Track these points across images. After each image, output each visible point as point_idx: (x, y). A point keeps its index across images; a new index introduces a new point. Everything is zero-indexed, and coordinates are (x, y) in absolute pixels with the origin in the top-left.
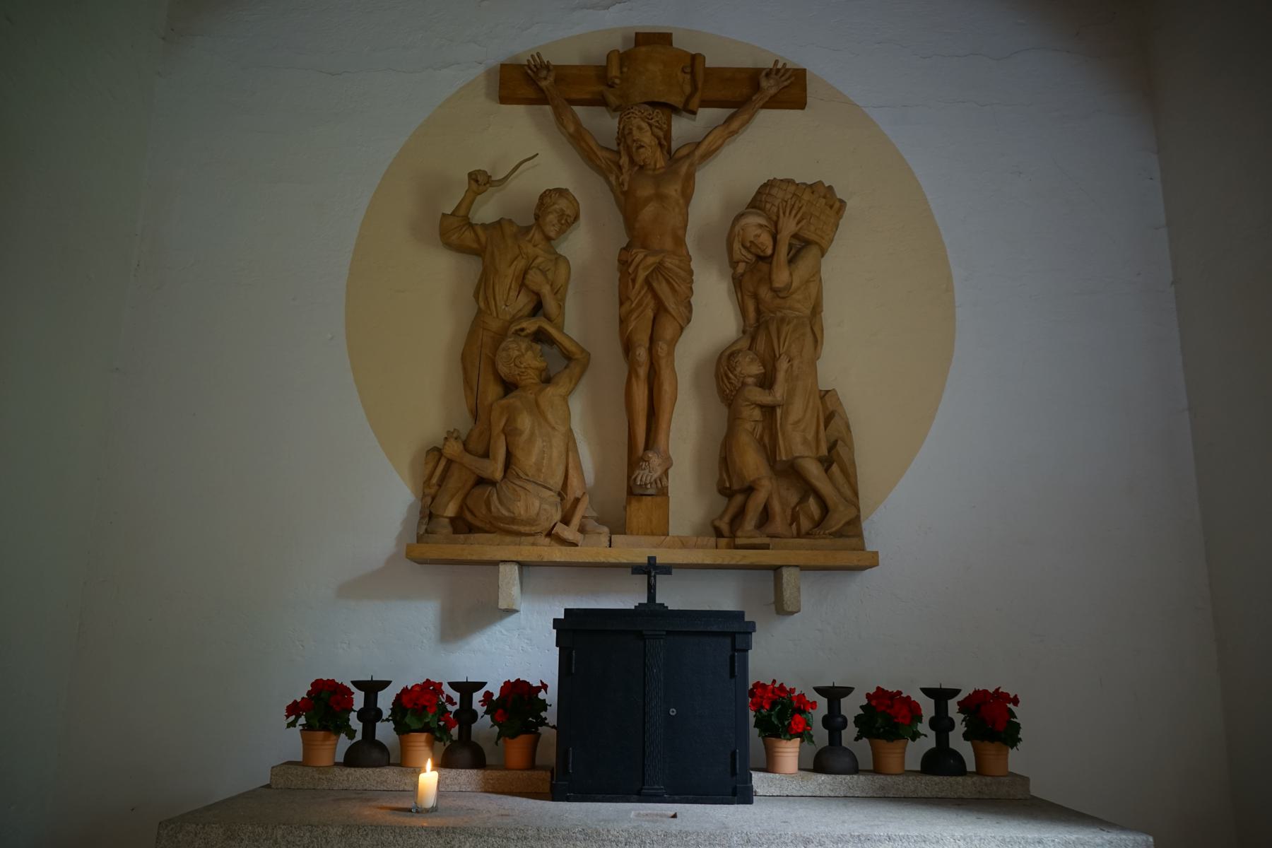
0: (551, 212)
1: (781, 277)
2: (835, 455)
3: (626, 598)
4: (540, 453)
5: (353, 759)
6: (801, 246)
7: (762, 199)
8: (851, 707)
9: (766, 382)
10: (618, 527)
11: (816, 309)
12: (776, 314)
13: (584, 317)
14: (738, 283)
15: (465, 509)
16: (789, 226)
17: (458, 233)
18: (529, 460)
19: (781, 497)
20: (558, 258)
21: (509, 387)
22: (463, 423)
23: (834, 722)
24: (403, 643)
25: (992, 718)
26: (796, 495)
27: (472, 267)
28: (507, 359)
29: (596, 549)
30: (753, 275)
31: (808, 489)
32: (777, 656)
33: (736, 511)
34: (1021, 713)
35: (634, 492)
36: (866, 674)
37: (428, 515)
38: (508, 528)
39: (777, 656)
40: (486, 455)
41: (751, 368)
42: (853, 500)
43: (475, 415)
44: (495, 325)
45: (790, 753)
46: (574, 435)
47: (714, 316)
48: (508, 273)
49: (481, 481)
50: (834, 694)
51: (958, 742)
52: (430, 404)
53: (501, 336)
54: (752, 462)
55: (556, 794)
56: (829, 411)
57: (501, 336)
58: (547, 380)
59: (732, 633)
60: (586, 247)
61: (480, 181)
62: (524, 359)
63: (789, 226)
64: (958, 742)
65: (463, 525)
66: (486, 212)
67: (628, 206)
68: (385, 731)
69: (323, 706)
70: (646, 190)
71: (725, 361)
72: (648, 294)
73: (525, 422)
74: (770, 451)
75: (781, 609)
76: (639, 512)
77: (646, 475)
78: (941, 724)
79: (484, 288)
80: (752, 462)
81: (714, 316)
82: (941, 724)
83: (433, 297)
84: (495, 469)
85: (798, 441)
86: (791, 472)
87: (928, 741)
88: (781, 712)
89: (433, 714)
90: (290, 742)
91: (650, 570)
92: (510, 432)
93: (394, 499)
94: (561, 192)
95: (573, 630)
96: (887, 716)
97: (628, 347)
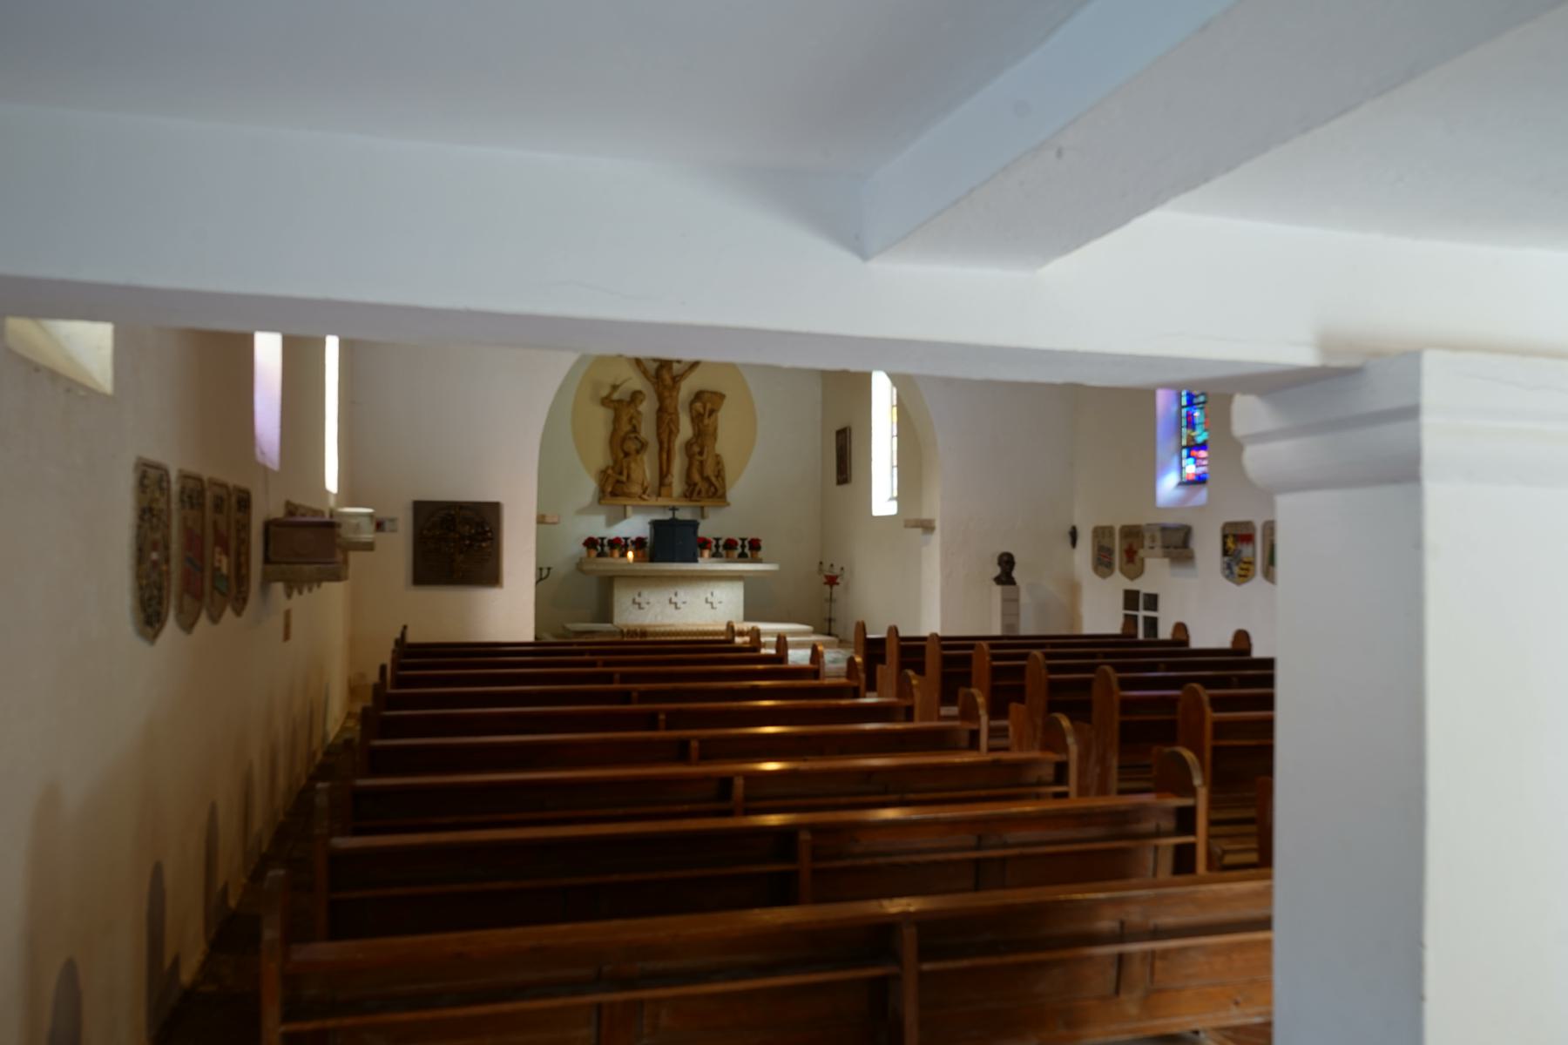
0: (636, 396)
1: (706, 421)
2: (720, 474)
3: (667, 516)
4: (636, 475)
5: (600, 555)
6: (712, 412)
7: (699, 396)
8: (721, 543)
9: (701, 453)
10: (659, 495)
11: (715, 429)
12: (703, 434)
13: (647, 430)
14: (693, 420)
15: (614, 488)
16: (709, 406)
17: (606, 401)
18: (634, 476)
19: (702, 486)
20: (639, 413)
21: (627, 454)
22: (611, 463)
23: (717, 546)
24: (598, 526)
25: (755, 545)
26: (708, 486)
27: (610, 413)
28: (623, 444)
29: (653, 501)
30: (697, 419)
31: (711, 484)
32: (703, 531)
33: (691, 492)
34: (763, 544)
35: (662, 484)
36: (725, 535)
37: (602, 491)
38: (628, 495)
39: (703, 531)
40: (621, 473)
41: (696, 449)
42: (724, 487)
43: (616, 461)
44: (622, 434)
45: (706, 553)
46: (645, 468)
47: (685, 430)
48: (625, 419)
49: (618, 482)
50: (717, 540)
51: (747, 550)
52: (600, 456)
53: (624, 440)
54: (696, 477)
55: (652, 560)
56: (718, 462)
57: (624, 440)
58: (638, 452)
59: (694, 525)
60: (647, 408)
61: (615, 388)
62: (631, 446)
63: (709, 406)
64: (747, 550)
65: (614, 494)
66: (616, 396)
67: (661, 398)
68: (607, 549)
69: (591, 543)
70: (666, 394)
71: (688, 445)
72: (665, 420)
73: (633, 465)
74: (701, 473)
75: (703, 517)
76: (664, 491)
77: (667, 481)
78: (743, 546)
79: (616, 420)
80: (696, 477)
81: (685, 430)
82: (743, 546)
83: (600, 421)
84: (624, 478)
85: (710, 471)
86: (707, 479)
87: (739, 550)
88: (704, 544)
89: (618, 545)
90: (584, 549)
91: (674, 509)
92: (629, 468)
93: (589, 487)
94: (640, 392)
95: (656, 525)
96: (730, 545)
97: (661, 443)
